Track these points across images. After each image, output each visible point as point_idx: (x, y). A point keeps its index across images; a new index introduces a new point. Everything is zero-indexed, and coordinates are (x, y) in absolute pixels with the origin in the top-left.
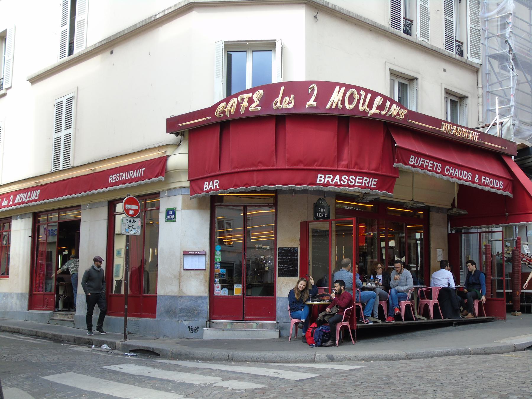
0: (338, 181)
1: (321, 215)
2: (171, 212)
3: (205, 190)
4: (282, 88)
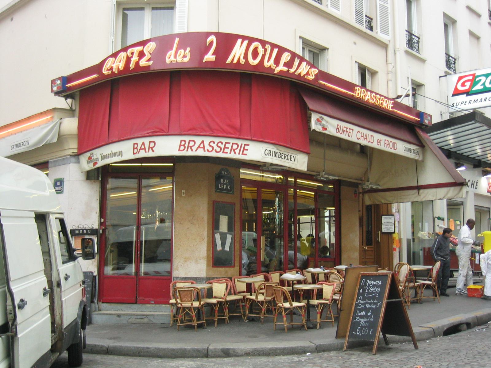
1: (223, 186)
2: (58, 183)
4: (177, 40)
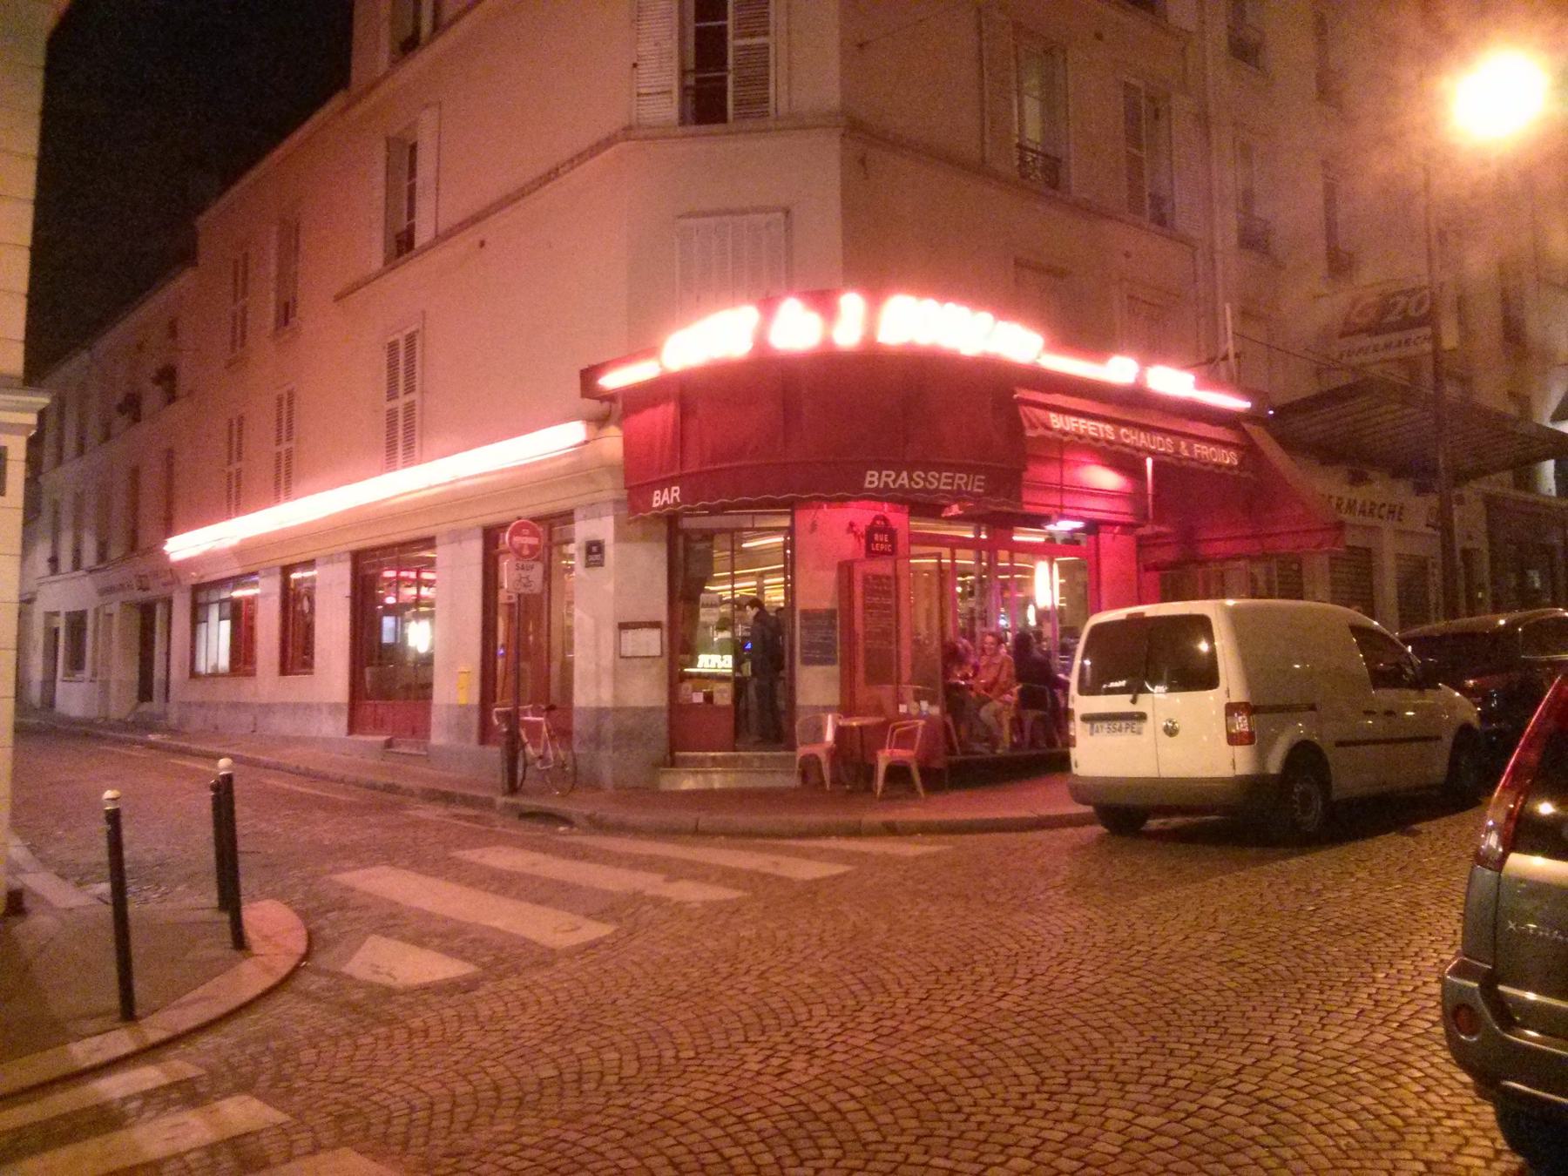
0: (906, 482)
2: (594, 549)
3: (655, 505)
